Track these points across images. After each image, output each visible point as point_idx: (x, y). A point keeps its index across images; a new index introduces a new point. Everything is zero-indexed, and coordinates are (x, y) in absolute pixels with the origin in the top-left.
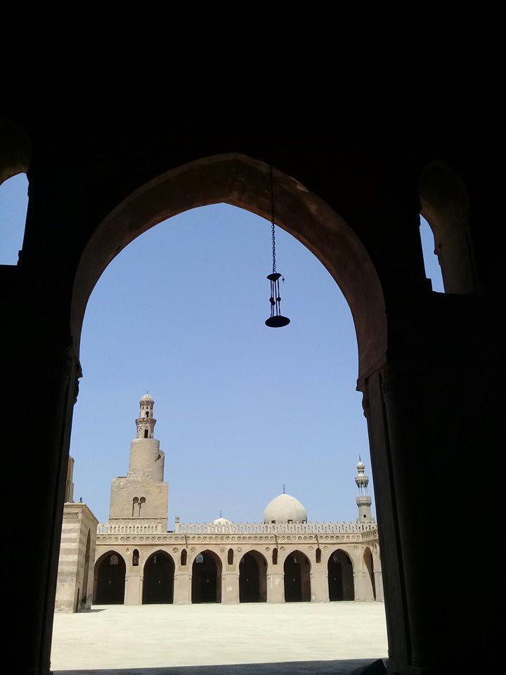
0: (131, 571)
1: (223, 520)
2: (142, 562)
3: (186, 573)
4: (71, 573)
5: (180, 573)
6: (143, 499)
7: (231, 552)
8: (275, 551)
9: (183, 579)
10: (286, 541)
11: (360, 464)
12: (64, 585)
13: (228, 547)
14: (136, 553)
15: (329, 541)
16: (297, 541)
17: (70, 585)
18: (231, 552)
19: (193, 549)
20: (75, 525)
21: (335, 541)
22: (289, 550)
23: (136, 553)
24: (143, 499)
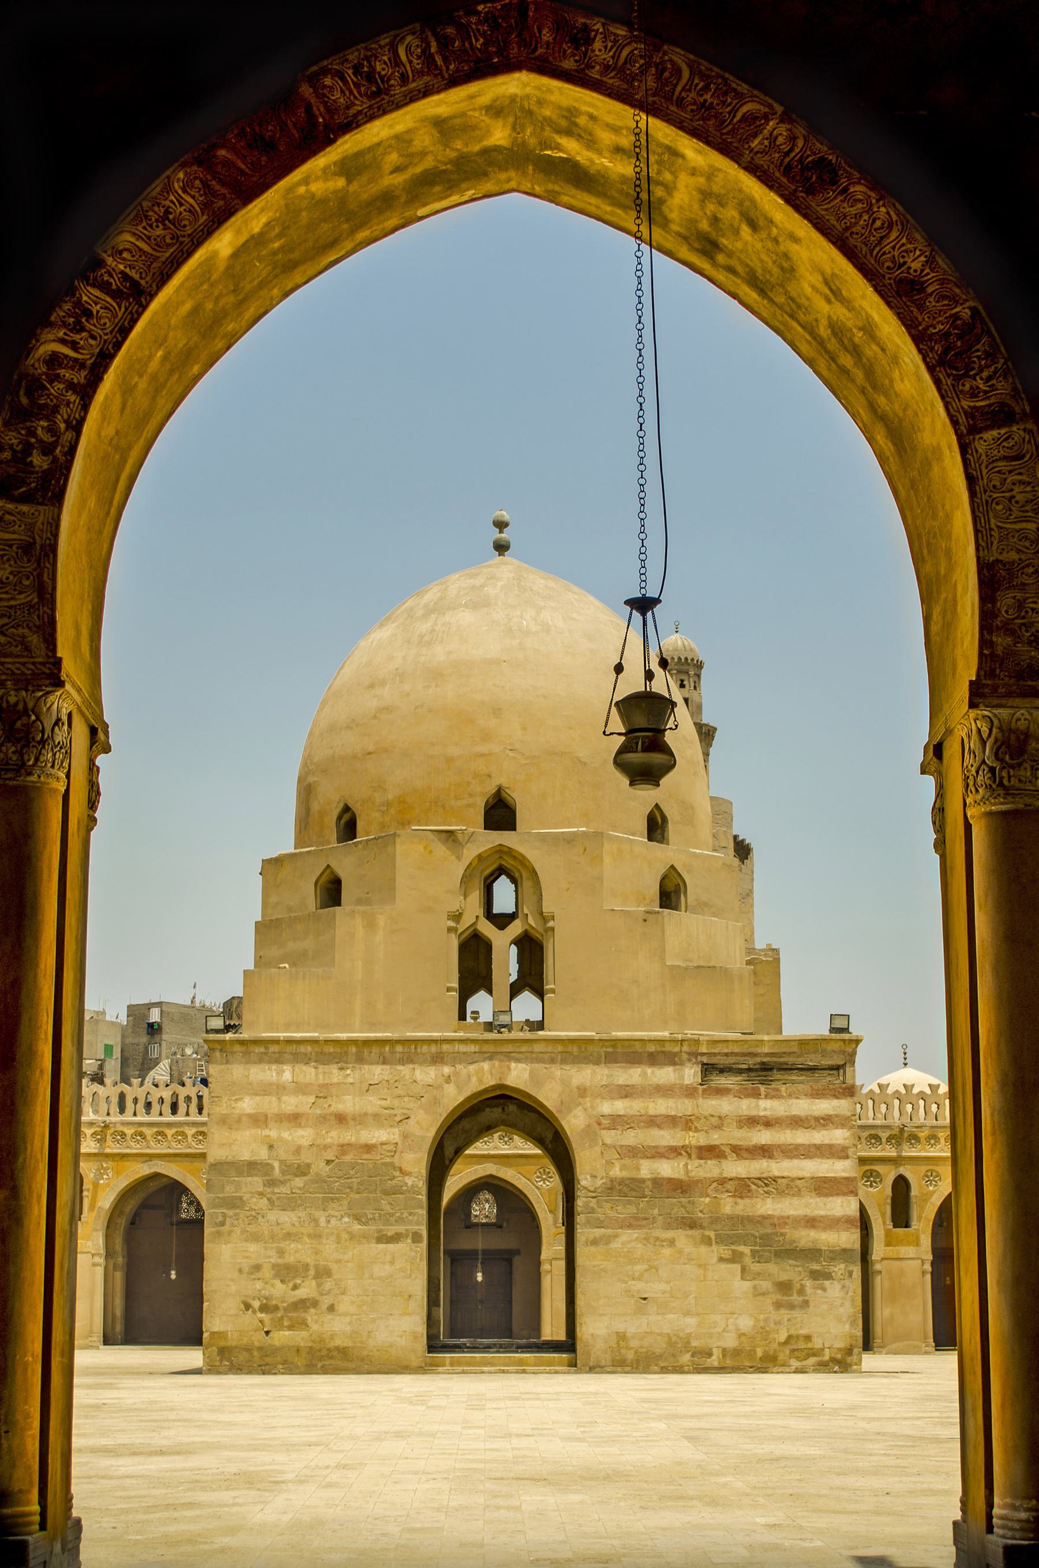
3: (909, 1251)
4: (844, 1254)
5: (891, 1251)
12: (824, 1290)
20: (835, 1102)
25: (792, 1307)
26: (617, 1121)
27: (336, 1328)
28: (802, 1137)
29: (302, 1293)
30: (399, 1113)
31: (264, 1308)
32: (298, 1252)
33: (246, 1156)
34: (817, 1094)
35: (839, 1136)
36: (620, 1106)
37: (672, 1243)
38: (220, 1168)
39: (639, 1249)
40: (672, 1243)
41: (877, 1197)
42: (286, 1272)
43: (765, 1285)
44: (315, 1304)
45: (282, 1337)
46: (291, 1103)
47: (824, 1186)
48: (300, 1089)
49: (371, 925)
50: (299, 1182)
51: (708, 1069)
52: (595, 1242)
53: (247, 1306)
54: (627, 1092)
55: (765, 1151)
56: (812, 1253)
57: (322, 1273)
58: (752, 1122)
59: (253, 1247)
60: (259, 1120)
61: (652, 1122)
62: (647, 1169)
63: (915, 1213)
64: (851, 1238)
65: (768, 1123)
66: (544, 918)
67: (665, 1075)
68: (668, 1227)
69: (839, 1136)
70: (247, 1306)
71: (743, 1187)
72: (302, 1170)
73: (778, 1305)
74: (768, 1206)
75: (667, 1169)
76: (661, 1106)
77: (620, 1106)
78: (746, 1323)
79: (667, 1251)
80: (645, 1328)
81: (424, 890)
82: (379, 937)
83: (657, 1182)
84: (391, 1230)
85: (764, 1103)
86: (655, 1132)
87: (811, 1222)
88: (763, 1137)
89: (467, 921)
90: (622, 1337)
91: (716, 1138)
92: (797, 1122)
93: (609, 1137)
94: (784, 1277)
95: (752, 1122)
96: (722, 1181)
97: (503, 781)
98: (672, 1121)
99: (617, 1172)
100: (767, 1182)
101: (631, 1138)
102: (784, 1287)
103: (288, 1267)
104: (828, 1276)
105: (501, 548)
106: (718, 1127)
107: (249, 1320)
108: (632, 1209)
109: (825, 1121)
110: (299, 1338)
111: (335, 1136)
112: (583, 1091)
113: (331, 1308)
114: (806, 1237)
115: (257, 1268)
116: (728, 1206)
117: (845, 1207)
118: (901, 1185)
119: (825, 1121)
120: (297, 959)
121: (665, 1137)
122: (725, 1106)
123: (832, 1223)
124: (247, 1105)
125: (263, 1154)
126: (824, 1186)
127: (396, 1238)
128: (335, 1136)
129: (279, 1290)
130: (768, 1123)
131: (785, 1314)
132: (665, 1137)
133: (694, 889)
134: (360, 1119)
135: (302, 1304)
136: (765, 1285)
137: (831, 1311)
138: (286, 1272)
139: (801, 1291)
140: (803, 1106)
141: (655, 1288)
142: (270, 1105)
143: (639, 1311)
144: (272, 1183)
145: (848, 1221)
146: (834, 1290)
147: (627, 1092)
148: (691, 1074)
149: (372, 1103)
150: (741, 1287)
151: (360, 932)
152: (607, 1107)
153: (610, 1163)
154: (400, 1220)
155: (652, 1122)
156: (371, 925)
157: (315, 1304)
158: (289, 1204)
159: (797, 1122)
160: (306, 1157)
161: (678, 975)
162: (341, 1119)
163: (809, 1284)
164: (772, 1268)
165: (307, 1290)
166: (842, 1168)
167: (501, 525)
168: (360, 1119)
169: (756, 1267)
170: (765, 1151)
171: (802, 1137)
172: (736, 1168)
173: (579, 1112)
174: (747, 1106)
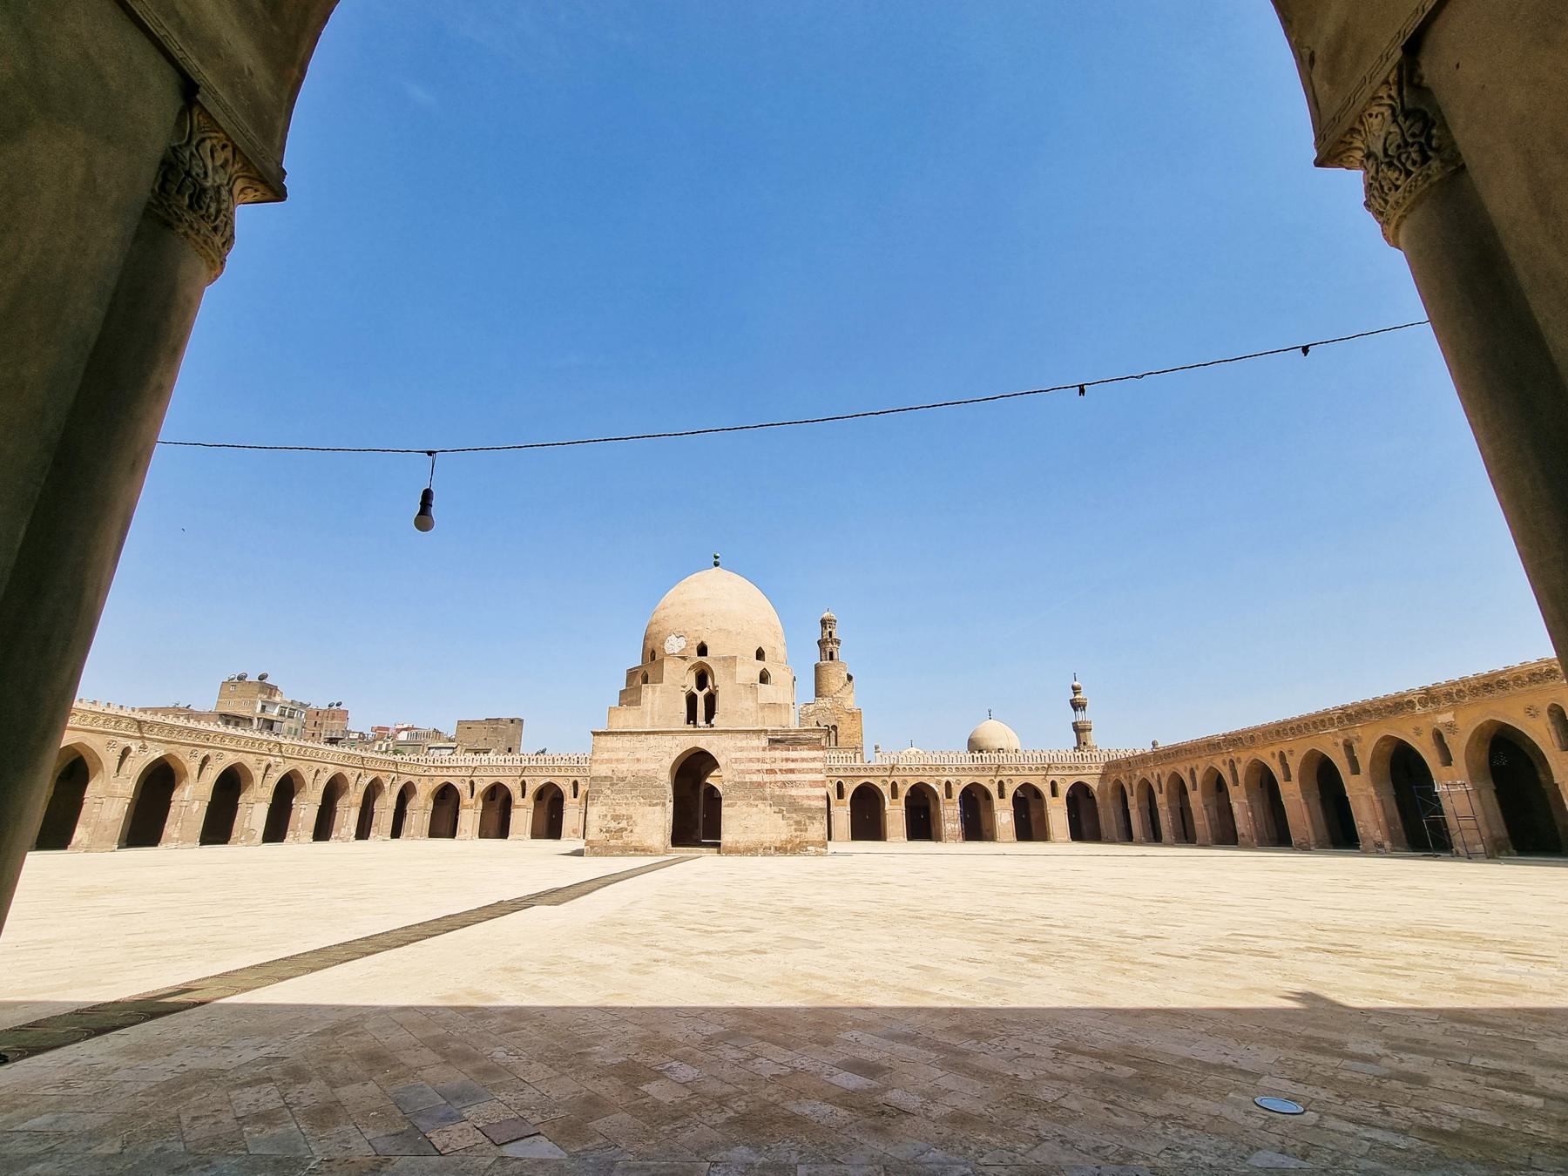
1: (913, 750)
2: (848, 798)
6: (835, 727)
7: (948, 784)
13: (944, 779)
14: (840, 785)
18: (948, 784)
19: (905, 782)
22: (1018, 782)
23: (840, 785)
24: (835, 727)
26: (737, 760)
27: (633, 839)
28: (805, 765)
32: (622, 810)
35: (818, 765)
36: (738, 755)
41: (832, 789)
42: (616, 818)
45: (612, 842)
46: (621, 755)
47: (814, 784)
48: (624, 749)
49: (654, 690)
54: (741, 749)
55: (792, 771)
56: (809, 809)
57: (629, 818)
58: (787, 760)
60: (609, 761)
61: (750, 760)
69: (818, 765)
71: (784, 784)
75: (756, 778)
76: (754, 755)
77: (738, 755)
78: (784, 837)
80: (744, 839)
81: (678, 678)
87: (808, 797)
88: (792, 765)
91: (774, 766)
92: (803, 760)
93: (735, 766)
95: (787, 760)
101: (742, 767)
102: (798, 823)
105: (716, 564)
107: (603, 836)
109: (814, 759)
110: (620, 842)
114: (806, 803)
116: (778, 791)
117: (822, 792)
119: (814, 759)
121: (756, 766)
122: (778, 754)
123: (817, 798)
124: (606, 756)
126: (814, 784)
128: (637, 766)
129: (613, 825)
132: (756, 766)
133: (772, 679)
135: (622, 830)
137: (817, 830)
138: (616, 818)
140: (806, 754)
142: (614, 756)
146: (817, 825)
147: (741, 749)
148: (764, 742)
155: (750, 760)
156: (654, 690)
158: (620, 792)
159: (803, 760)
161: (763, 707)
165: (624, 824)
166: (820, 777)
170: (792, 771)
171: (805, 765)
172: (780, 777)
174: (785, 754)
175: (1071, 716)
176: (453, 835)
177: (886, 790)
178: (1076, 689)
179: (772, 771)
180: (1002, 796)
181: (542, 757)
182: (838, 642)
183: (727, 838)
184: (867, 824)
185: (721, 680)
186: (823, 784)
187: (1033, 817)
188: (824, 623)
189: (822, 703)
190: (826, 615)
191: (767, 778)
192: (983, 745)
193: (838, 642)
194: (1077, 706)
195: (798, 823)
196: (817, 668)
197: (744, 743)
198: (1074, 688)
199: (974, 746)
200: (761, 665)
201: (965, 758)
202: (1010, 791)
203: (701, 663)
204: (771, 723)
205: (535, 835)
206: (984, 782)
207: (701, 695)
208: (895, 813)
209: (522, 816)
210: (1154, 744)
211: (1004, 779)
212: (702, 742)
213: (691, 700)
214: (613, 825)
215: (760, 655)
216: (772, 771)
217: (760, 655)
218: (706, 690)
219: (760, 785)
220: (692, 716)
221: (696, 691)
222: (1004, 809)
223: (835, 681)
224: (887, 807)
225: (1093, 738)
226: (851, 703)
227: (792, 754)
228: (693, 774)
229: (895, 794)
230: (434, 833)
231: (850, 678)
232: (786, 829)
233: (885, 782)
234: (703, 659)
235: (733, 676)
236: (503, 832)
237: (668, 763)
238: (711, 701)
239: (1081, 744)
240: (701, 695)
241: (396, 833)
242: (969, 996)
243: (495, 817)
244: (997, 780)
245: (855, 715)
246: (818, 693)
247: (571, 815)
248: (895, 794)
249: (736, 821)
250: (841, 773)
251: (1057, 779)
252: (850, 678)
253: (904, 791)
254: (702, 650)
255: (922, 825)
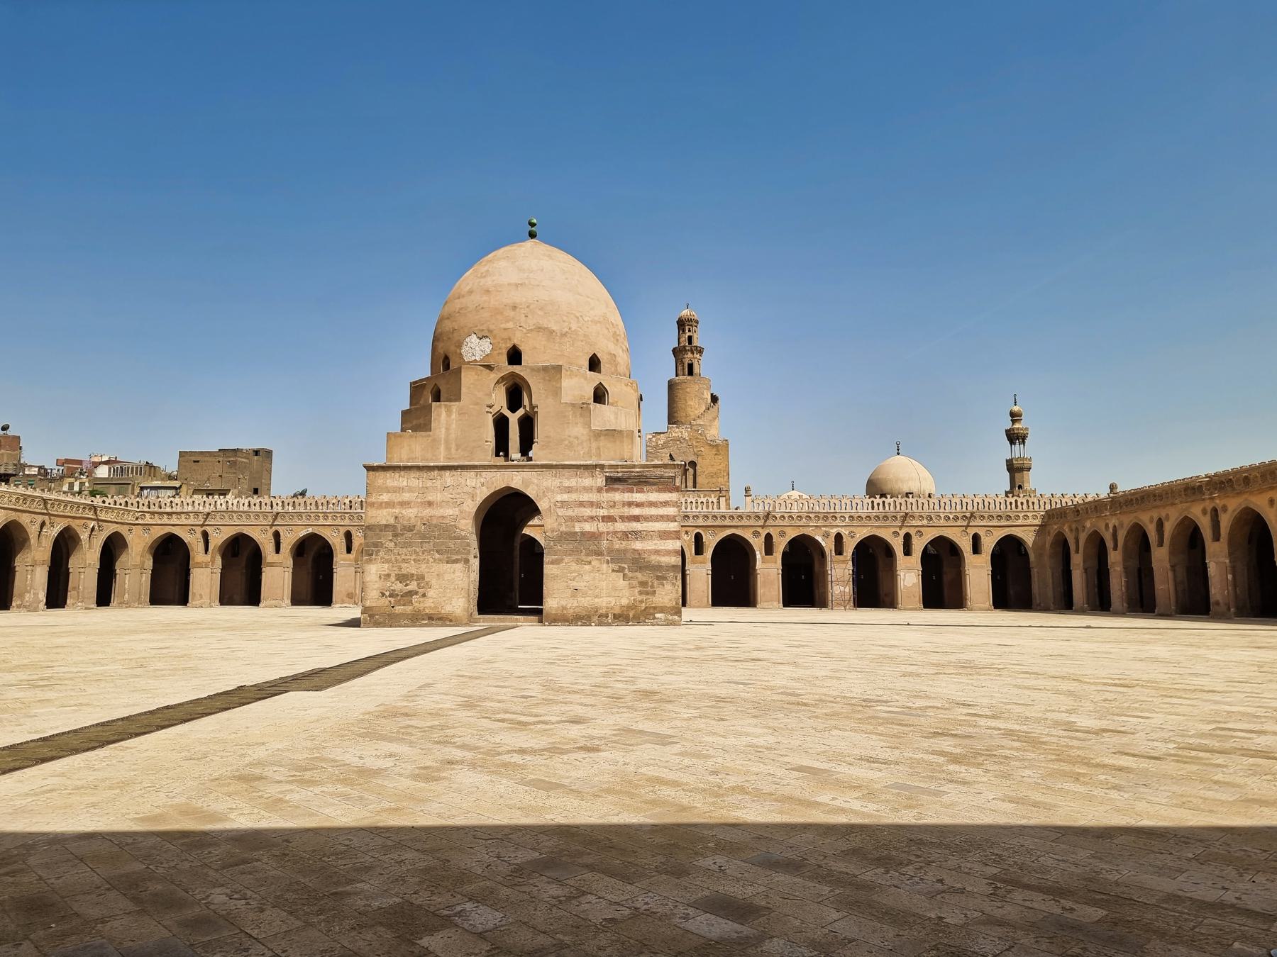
0: (693, 562)
1: (795, 494)
2: (709, 553)
3: (773, 565)
7: (839, 538)
8: (907, 538)
9: (768, 572)
10: (925, 522)
11: (1016, 409)
13: (834, 531)
14: (698, 538)
15: (995, 523)
16: (942, 522)
17: (674, 585)
18: (839, 538)
19: (782, 534)
21: (1003, 523)
22: (930, 535)
23: (698, 538)
24: (693, 464)
25: (647, 594)
26: (563, 504)
27: (427, 605)
29: (409, 588)
30: (460, 501)
31: (391, 596)
32: (409, 568)
33: (384, 522)
34: (660, 491)
35: (671, 511)
36: (565, 497)
37: (590, 563)
38: (370, 528)
39: (574, 566)
40: (590, 563)
41: (688, 541)
42: (403, 578)
43: (635, 583)
44: (416, 593)
45: (399, 609)
46: (406, 496)
47: (664, 535)
48: (411, 490)
50: (409, 534)
51: (610, 480)
52: (552, 563)
53: (383, 594)
54: (569, 490)
55: (636, 518)
56: (658, 567)
57: (420, 578)
58: (630, 504)
59: (386, 566)
60: (390, 505)
61: (581, 504)
62: (577, 528)
63: (775, 549)
64: (677, 560)
65: (638, 505)
66: (532, 407)
67: (587, 481)
68: (587, 555)
69: (671, 511)
70: (383, 594)
71: (625, 535)
72: (411, 529)
73: (641, 593)
74: (638, 545)
75: (588, 527)
76: (586, 497)
77: (565, 497)
78: (625, 602)
79: (587, 567)
80: (573, 605)
81: (482, 395)
82: (453, 416)
83: (583, 534)
84: (455, 557)
85: (638, 495)
86: (583, 509)
87: (657, 552)
88: (636, 511)
89: (496, 409)
90: (564, 608)
91: (612, 512)
93: (561, 512)
94: (644, 579)
95: (630, 504)
96: (615, 533)
97: (516, 341)
98: (591, 504)
99: (563, 529)
100: (637, 535)
101: (570, 513)
102: (643, 584)
103: (404, 575)
104: (665, 579)
106: (613, 507)
107: (384, 602)
108: (571, 546)
109: (666, 504)
110: (409, 609)
111: (428, 512)
112: (548, 489)
113: (424, 595)
114: (654, 559)
115: (388, 575)
116: (618, 544)
117: (677, 545)
118: (769, 538)
119: (666, 504)
120: (415, 429)
121: (588, 512)
122: (618, 496)
123: (668, 553)
124: (385, 497)
125: (392, 521)
126: (664, 535)
127: (456, 561)
128: (428, 512)
129: (399, 587)
130: (638, 505)
131: (644, 597)
132: (588, 512)
134: (442, 504)
135: (411, 593)
136: (635, 583)
137: (667, 593)
138: (403, 578)
139: (652, 587)
140: (654, 496)
141: (580, 585)
142: (396, 498)
143: (573, 596)
144: (395, 536)
145: (676, 552)
146: (668, 587)
147: (569, 490)
148: (600, 481)
149: (447, 496)
150: (622, 583)
151: (444, 415)
152: (559, 498)
153: (560, 524)
154: (458, 553)
155: (581, 504)
157: (416, 593)
158: (406, 545)
160: (413, 521)
161: (598, 435)
162: (430, 504)
163: (656, 582)
164: (639, 575)
165: (413, 586)
166: (673, 526)
167: (533, 225)
168: (442, 504)
169: (630, 574)
170: (636, 518)
172: (621, 526)
173: (546, 500)
174: (627, 497)
175: (1005, 451)
176: (183, 600)
177: (758, 544)
178: (1015, 416)
179: (609, 519)
180: (908, 551)
181: (300, 500)
182: (700, 351)
183: (551, 603)
184: (733, 586)
185: (539, 397)
186: (676, 535)
187: (947, 578)
188: (682, 324)
189: (677, 432)
190: (685, 313)
191: (603, 527)
192: (887, 488)
193: (700, 351)
194: (1014, 437)
195: (643, 584)
196: (672, 386)
197: (572, 482)
198: (1013, 414)
199: (875, 488)
200: (595, 379)
201: (863, 504)
202: (918, 545)
203: (513, 375)
204: (609, 456)
205: (297, 600)
206: (885, 534)
207: (514, 419)
208: (769, 573)
209: (278, 575)
210: (1112, 487)
211: (912, 532)
212: (517, 480)
213: (501, 424)
214: (399, 587)
215: (594, 364)
216: (609, 519)
217: (594, 364)
218: (521, 412)
219: (594, 536)
220: (502, 446)
221: (507, 413)
222: (909, 569)
223: (694, 405)
224: (759, 565)
225: (1033, 480)
226: (715, 432)
227: (638, 497)
228: (505, 519)
229: (769, 549)
230: (157, 598)
231: (714, 399)
232: (626, 592)
233: (756, 534)
234: (516, 369)
235: (557, 392)
236: (253, 597)
237: (471, 507)
238: (527, 425)
239: (1016, 486)
240: (514, 419)
241: (104, 598)
242: (872, 807)
243: (239, 577)
244: (902, 532)
245: (720, 448)
246: (672, 419)
247: (343, 574)
248: (769, 549)
249: (562, 582)
250: (701, 522)
251: (981, 532)
252: (714, 399)
253: (780, 545)
254: (515, 356)
255: (803, 587)
